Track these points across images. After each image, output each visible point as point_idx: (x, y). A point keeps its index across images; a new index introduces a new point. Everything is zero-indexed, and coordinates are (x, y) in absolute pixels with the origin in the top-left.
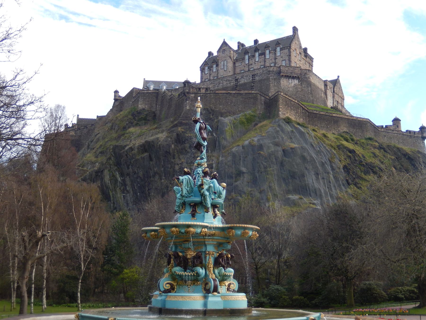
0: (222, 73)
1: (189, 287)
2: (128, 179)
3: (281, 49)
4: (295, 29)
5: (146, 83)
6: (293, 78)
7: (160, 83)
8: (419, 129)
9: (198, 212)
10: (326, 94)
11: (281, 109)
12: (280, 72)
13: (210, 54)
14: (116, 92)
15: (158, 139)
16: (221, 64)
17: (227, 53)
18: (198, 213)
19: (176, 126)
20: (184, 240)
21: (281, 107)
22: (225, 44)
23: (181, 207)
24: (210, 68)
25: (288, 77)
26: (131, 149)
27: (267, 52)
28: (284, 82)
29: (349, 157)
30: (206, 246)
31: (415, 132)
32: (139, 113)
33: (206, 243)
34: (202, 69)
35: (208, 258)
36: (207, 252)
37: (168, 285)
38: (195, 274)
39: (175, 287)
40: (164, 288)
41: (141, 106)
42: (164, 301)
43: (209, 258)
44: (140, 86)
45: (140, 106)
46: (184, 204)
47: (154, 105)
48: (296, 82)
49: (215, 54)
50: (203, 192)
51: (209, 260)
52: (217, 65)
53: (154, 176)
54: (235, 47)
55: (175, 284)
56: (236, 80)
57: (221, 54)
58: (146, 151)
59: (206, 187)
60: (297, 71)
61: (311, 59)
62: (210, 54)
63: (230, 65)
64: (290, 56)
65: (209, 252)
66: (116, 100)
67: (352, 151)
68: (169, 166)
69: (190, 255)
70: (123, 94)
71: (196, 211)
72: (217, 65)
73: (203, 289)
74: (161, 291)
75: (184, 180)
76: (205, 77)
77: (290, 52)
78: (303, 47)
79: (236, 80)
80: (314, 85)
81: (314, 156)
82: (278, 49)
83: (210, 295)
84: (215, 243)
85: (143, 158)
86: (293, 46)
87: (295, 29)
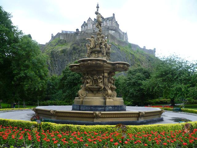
0: (88, 28)
2: (56, 62)
3: (109, 21)
4: (114, 14)
5: (62, 31)
6: (113, 30)
7: (67, 31)
10: (123, 36)
12: (109, 28)
13: (85, 22)
14: (52, 34)
15: (67, 48)
16: (88, 25)
17: (91, 22)
19: (73, 44)
22: (90, 18)
24: (84, 27)
25: (112, 30)
26: (58, 52)
27: (104, 22)
28: (110, 32)
29: (132, 57)
32: (61, 40)
34: (82, 27)
35: (105, 79)
41: (61, 38)
42: (82, 102)
44: (61, 32)
45: (60, 38)
46: (91, 53)
47: (66, 38)
48: (114, 31)
49: (86, 22)
52: (87, 26)
53: (65, 61)
54: (93, 20)
56: (94, 30)
57: (88, 22)
58: (63, 53)
59: (103, 44)
60: (114, 28)
61: (118, 25)
62: (85, 22)
63: (92, 26)
64: (112, 23)
66: (52, 37)
67: (133, 55)
68: (71, 58)
70: (54, 35)
72: (87, 26)
75: (92, 41)
76: (83, 30)
77: (112, 22)
78: (116, 21)
79: (94, 30)
80: (120, 33)
81: (121, 55)
82: (108, 21)
85: (62, 55)
86: (113, 20)
87: (114, 14)
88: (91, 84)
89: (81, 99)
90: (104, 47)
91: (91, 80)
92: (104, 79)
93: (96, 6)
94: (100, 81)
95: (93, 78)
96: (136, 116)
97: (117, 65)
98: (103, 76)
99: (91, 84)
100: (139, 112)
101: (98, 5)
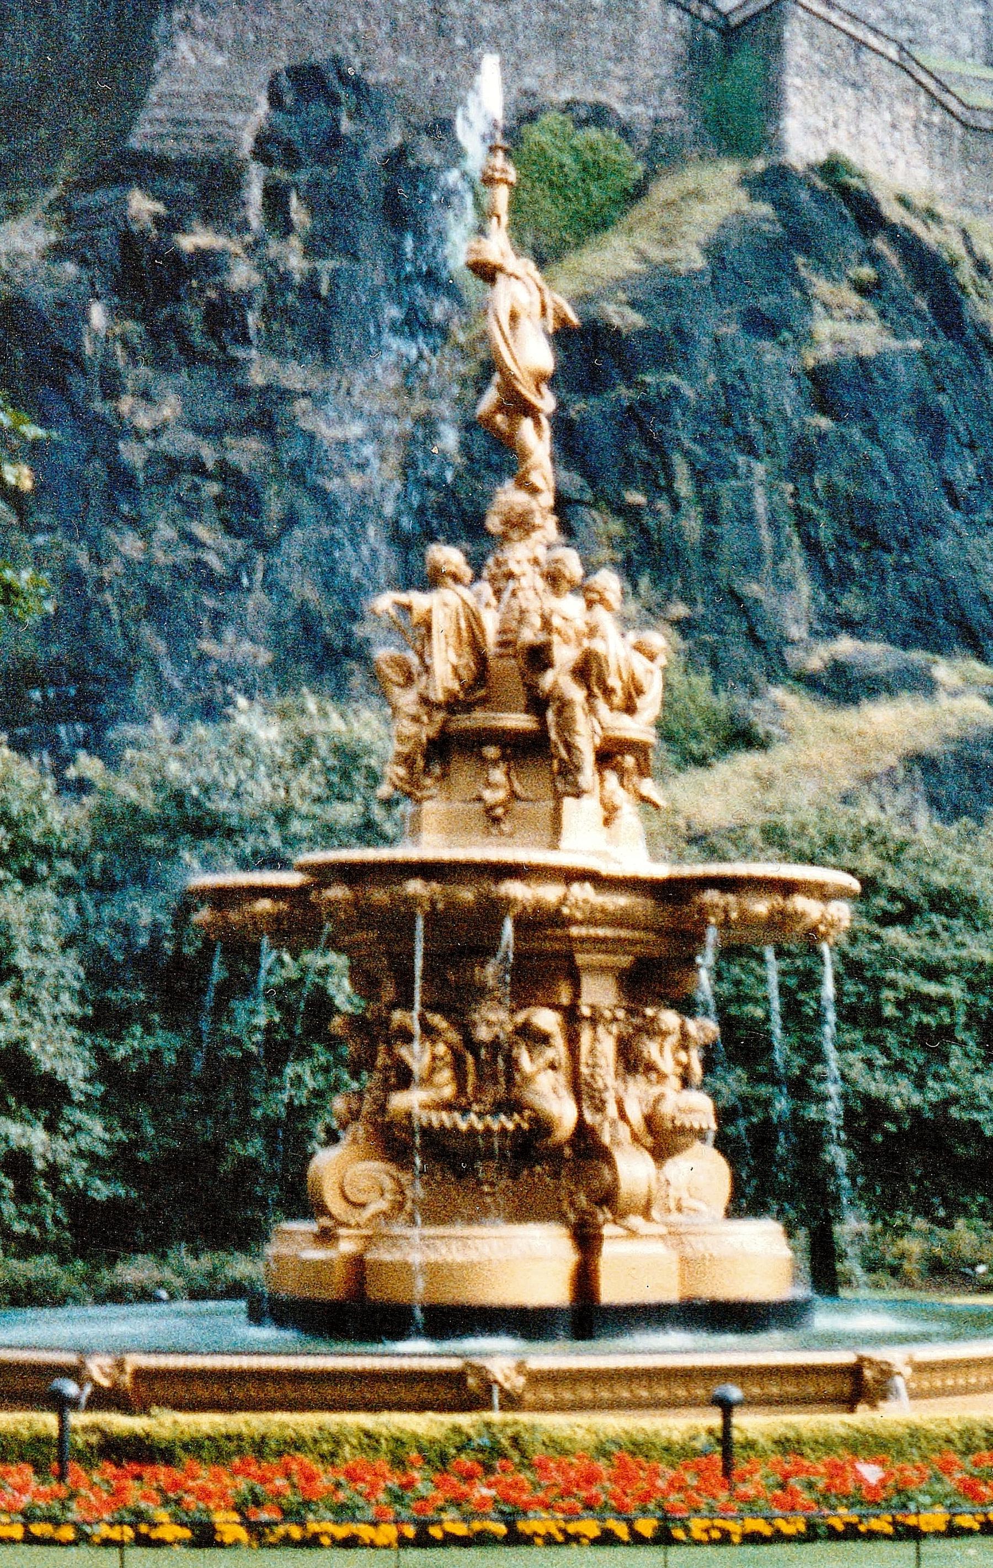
11: (793, 100)
21: (798, 82)
23: (420, 763)
30: (574, 979)
33: (581, 959)
36: (586, 1011)
38: (525, 1126)
43: (595, 1039)
50: (556, 683)
51: (592, 1051)
65: (593, 1007)
69: (489, 1024)
84: (625, 961)
88: (448, 1092)
89: (347, 1247)
90: (576, 694)
91: (441, 1049)
92: (573, 1041)
94: (541, 1062)
95: (465, 1029)
96: (830, 1389)
97: (711, 896)
98: (571, 1016)
99: (448, 1092)
100: (861, 1359)
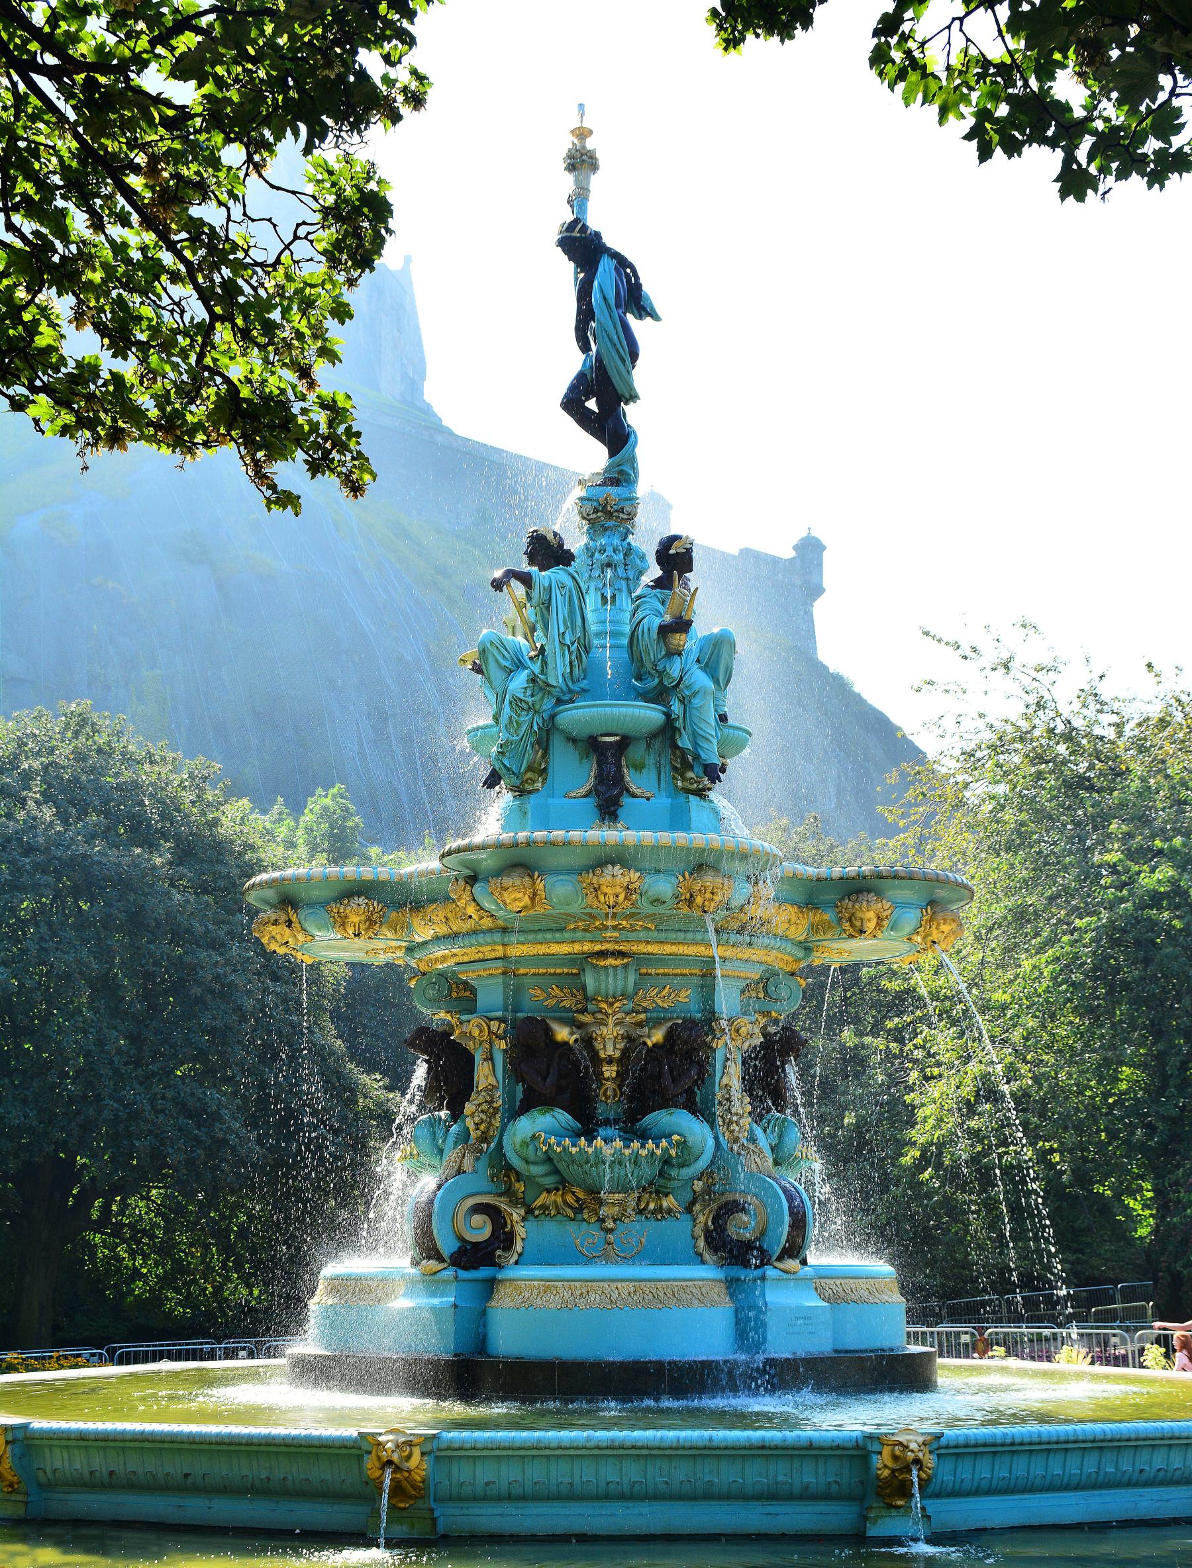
1: (610, 1231)
8: (795, 548)
9: (633, 788)
18: (634, 796)
20: (598, 948)
31: (775, 561)
37: (478, 1219)
39: (520, 1231)
40: (461, 1239)
55: (516, 1214)
71: (619, 780)
73: (701, 1243)
74: (440, 1259)
83: (770, 1272)
93: (567, 143)
101: (582, 134)
